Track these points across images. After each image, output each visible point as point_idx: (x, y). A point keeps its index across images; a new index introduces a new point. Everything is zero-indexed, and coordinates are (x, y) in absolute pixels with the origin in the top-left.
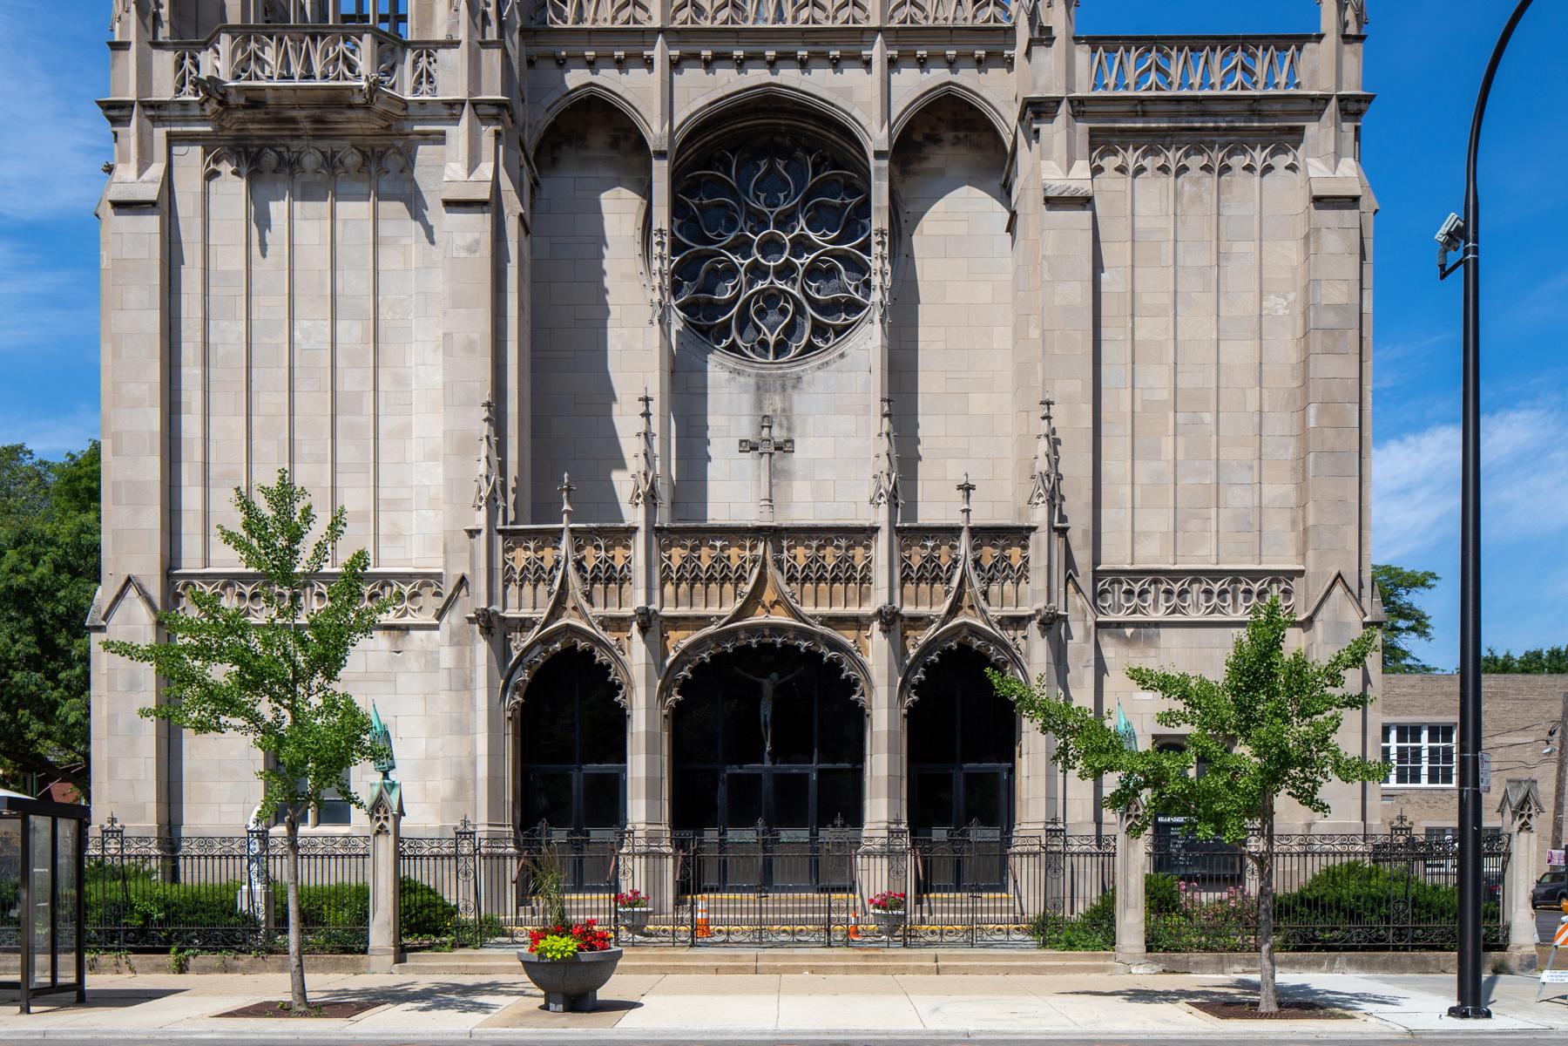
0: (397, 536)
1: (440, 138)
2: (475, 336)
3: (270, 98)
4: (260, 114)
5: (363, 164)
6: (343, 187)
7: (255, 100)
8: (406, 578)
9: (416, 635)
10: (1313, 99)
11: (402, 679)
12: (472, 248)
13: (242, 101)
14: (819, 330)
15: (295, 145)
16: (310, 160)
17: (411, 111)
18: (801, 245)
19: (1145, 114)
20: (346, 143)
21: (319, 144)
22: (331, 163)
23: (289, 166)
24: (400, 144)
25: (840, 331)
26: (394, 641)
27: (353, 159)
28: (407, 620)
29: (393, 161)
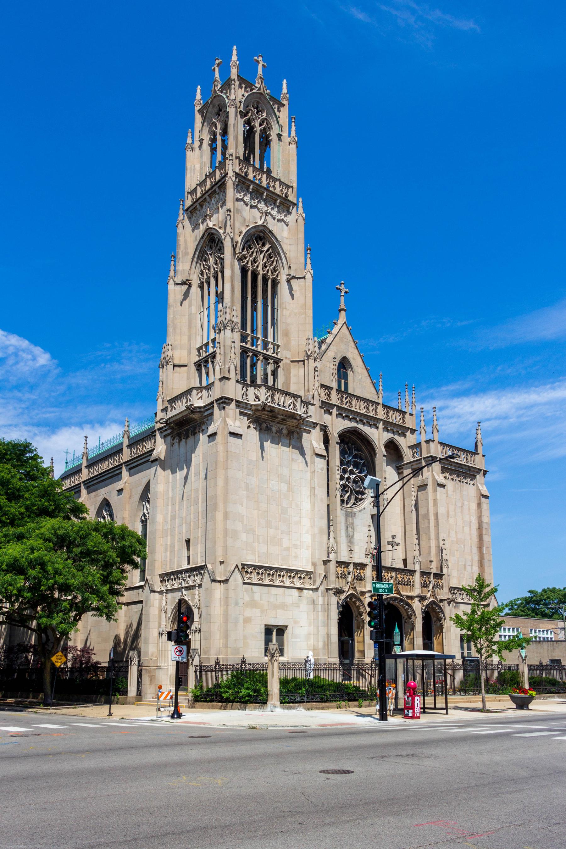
0: (296, 557)
1: (309, 432)
2: (323, 497)
3: (276, 411)
4: (270, 414)
5: (288, 434)
6: (283, 440)
7: (272, 410)
8: (302, 572)
9: (305, 591)
10: (479, 469)
11: (302, 606)
12: (322, 470)
13: (269, 410)
14: (356, 499)
15: (272, 423)
16: (274, 429)
17: (305, 422)
18: (352, 472)
19: (451, 465)
20: (285, 427)
21: (279, 425)
22: (280, 431)
23: (268, 429)
24: (298, 431)
25: (361, 500)
26: (300, 593)
27: (285, 432)
28: (302, 586)
29: (295, 435)
